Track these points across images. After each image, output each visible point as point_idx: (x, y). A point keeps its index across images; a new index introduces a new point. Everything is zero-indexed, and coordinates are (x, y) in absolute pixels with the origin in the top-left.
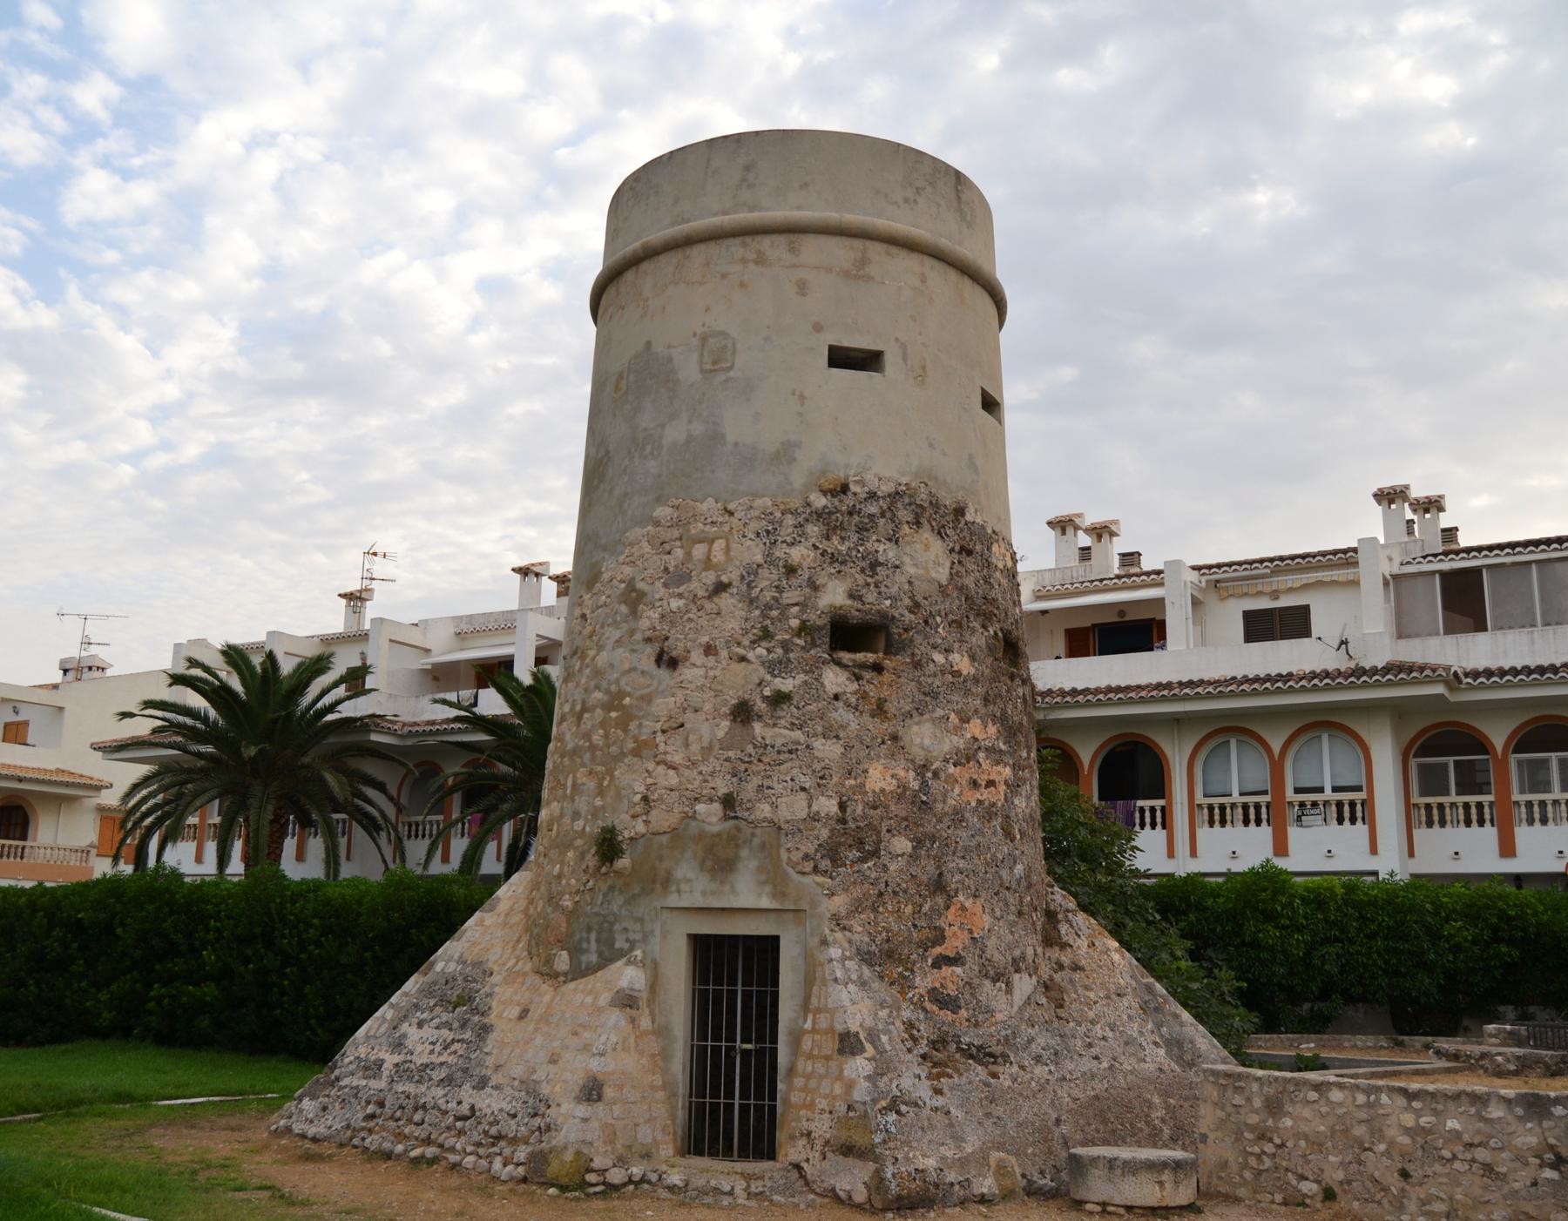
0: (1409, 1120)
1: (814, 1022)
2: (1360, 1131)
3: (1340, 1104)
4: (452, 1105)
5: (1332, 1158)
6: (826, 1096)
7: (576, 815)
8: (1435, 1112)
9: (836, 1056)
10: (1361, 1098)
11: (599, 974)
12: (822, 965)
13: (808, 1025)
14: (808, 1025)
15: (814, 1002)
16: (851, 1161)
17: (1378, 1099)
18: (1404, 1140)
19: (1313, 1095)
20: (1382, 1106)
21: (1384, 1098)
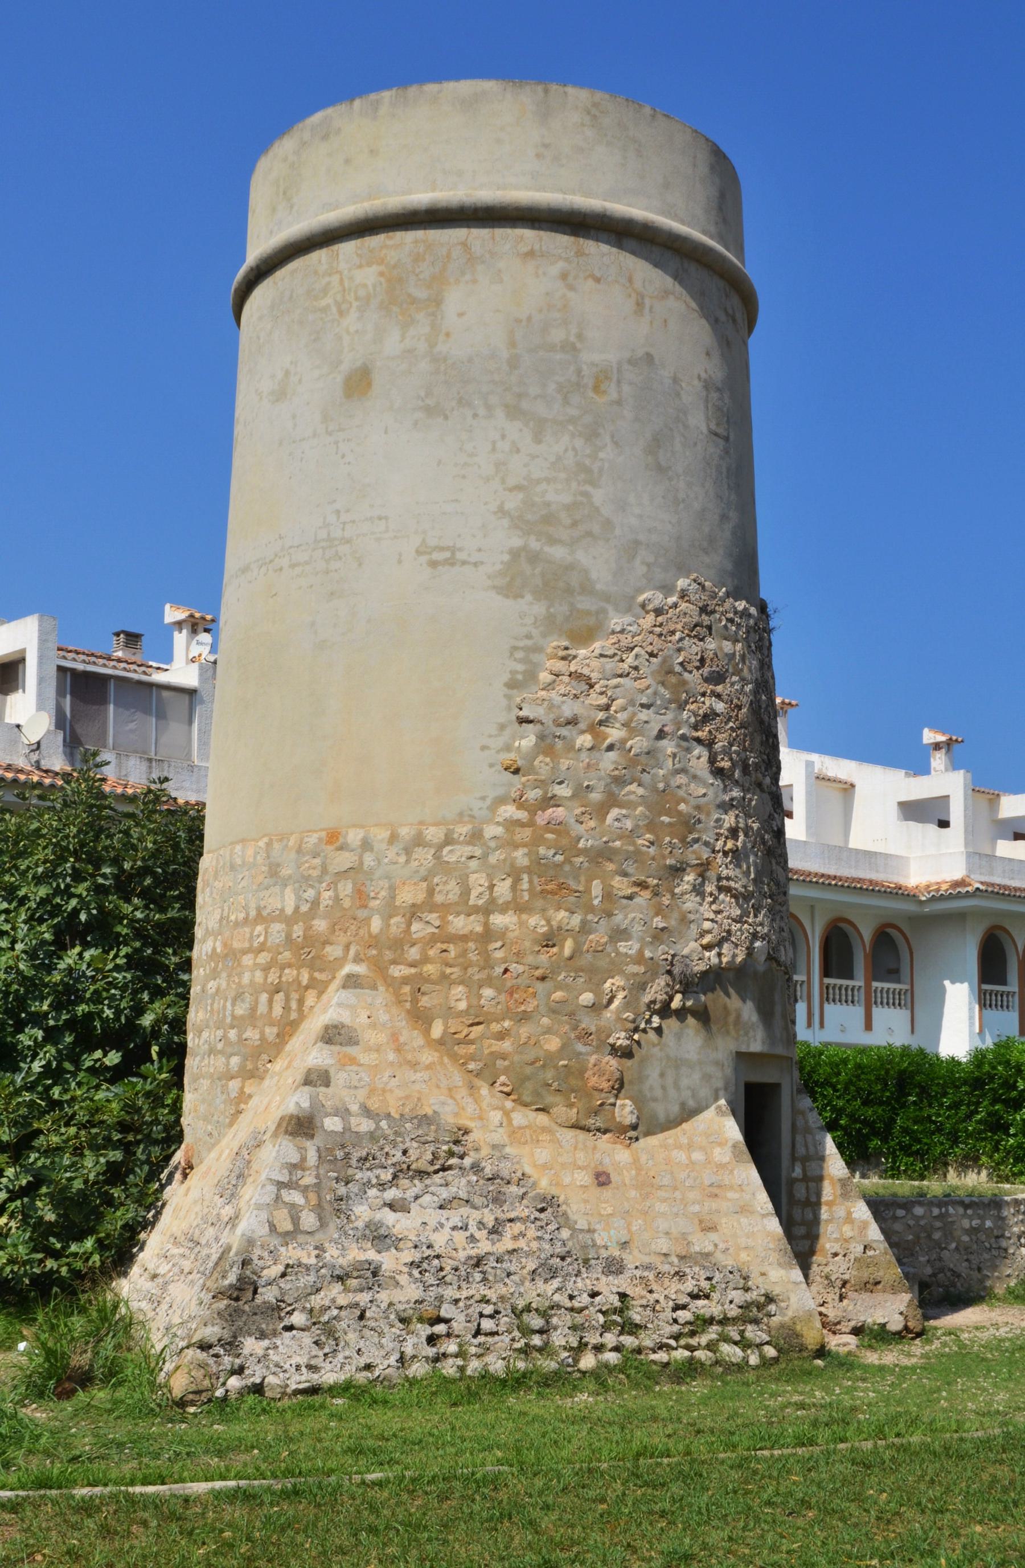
0: (966, 1224)
1: (804, 1170)
2: (937, 1236)
3: (922, 1217)
4: (585, 1299)
5: (922, 1259)
6: (837, 1240)
7: (620, 934)
8: (980, 1217)
9: (839, 1200)
10: (936, 1211)
11: (684, 1125)
12: (803, 1113)
13: (798, 1172)
14: (798, 1172)
15: (801, 1151)
16: (879, 1297)
17: (947, 1210)
18: (966, 1238)
19: (901, 1213)
20: (950, 1215)
21: (951, 1210)
